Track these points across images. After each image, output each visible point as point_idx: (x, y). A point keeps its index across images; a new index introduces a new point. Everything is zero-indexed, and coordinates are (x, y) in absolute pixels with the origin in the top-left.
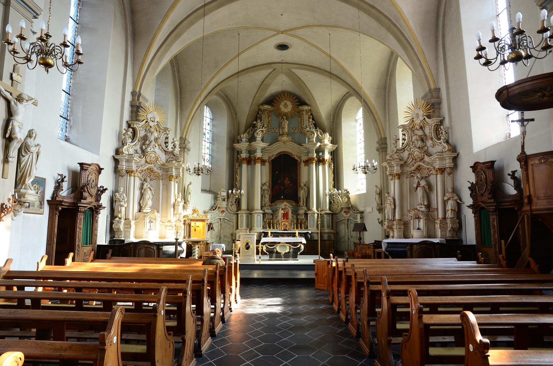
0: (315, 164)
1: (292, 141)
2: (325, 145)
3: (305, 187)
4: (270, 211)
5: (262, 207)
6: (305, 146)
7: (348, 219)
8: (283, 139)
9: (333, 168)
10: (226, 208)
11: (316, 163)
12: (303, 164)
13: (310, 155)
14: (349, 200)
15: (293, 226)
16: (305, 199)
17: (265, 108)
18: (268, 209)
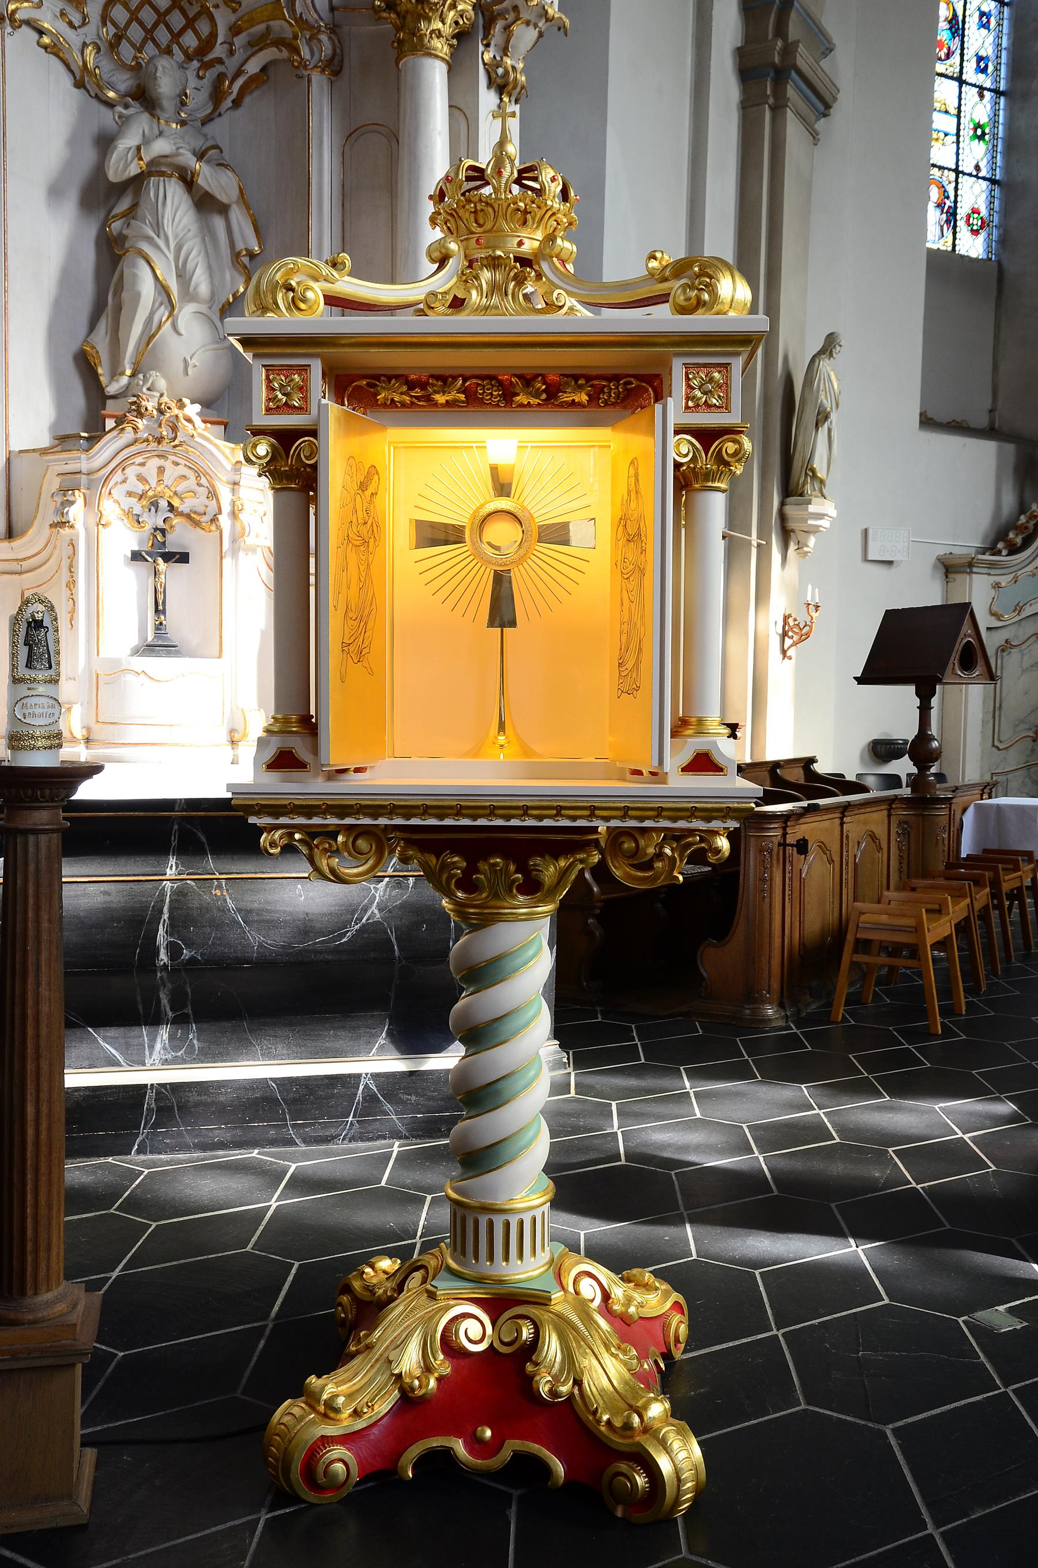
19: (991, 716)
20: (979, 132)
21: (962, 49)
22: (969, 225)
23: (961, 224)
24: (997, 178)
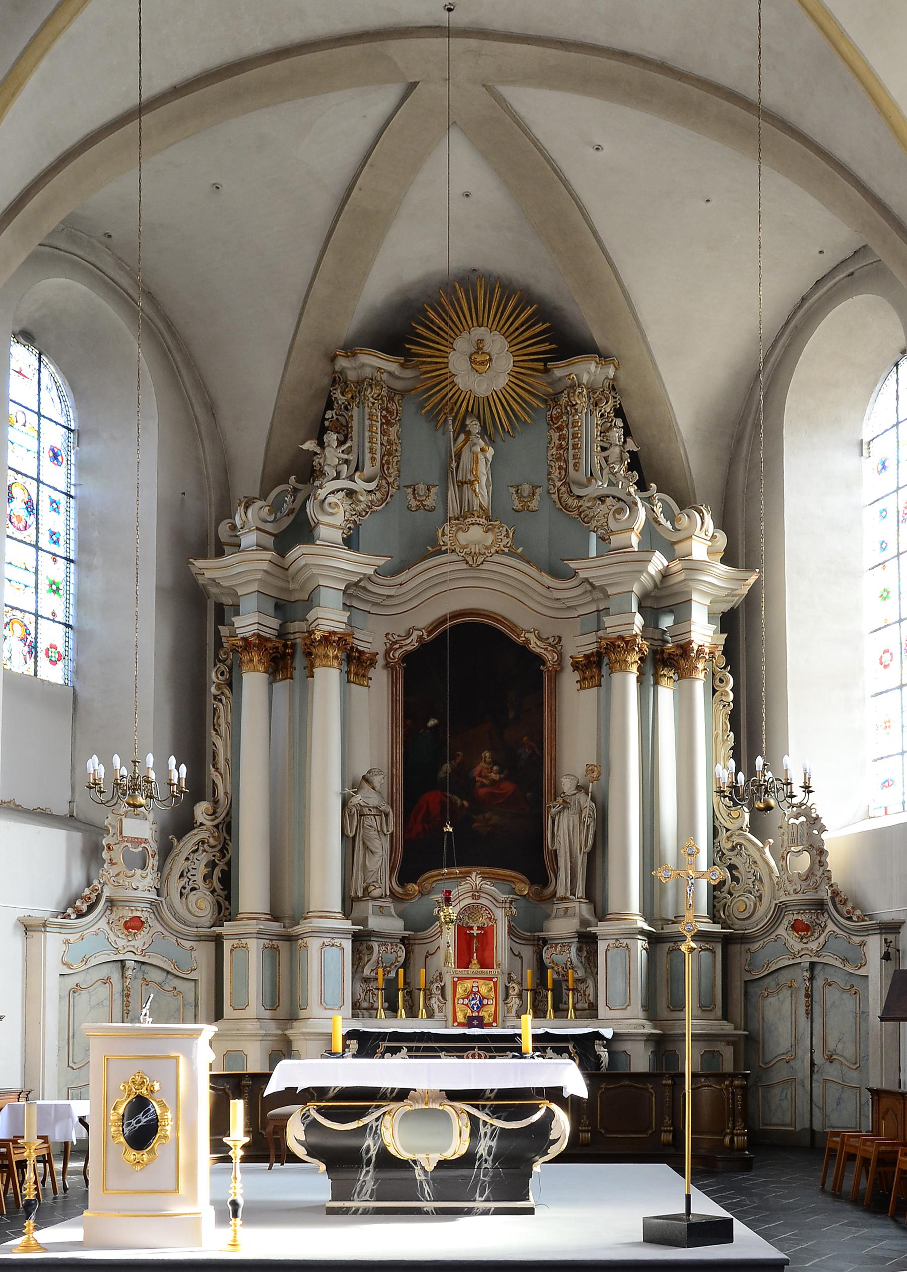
0: (634, 668)
2: (694, 568)
3: (582, 797)
4: (394, 925)
5: (349, 903)
6: (582, 574)
7: (813, 965)
9: (731, 696)
10: (155, 906)
11: (639, 669)
12: (570, 679)
13: (608, 621)
14: (822, 864)
15: (515, 1002)
16: (581, 861)
17: (368, 372)
18: (381, 912)
19: (66, 1042)
20: (54, 587)
21: (37, 524)
22: (48, 656)
23: (41, 655)
24: (70, 624)
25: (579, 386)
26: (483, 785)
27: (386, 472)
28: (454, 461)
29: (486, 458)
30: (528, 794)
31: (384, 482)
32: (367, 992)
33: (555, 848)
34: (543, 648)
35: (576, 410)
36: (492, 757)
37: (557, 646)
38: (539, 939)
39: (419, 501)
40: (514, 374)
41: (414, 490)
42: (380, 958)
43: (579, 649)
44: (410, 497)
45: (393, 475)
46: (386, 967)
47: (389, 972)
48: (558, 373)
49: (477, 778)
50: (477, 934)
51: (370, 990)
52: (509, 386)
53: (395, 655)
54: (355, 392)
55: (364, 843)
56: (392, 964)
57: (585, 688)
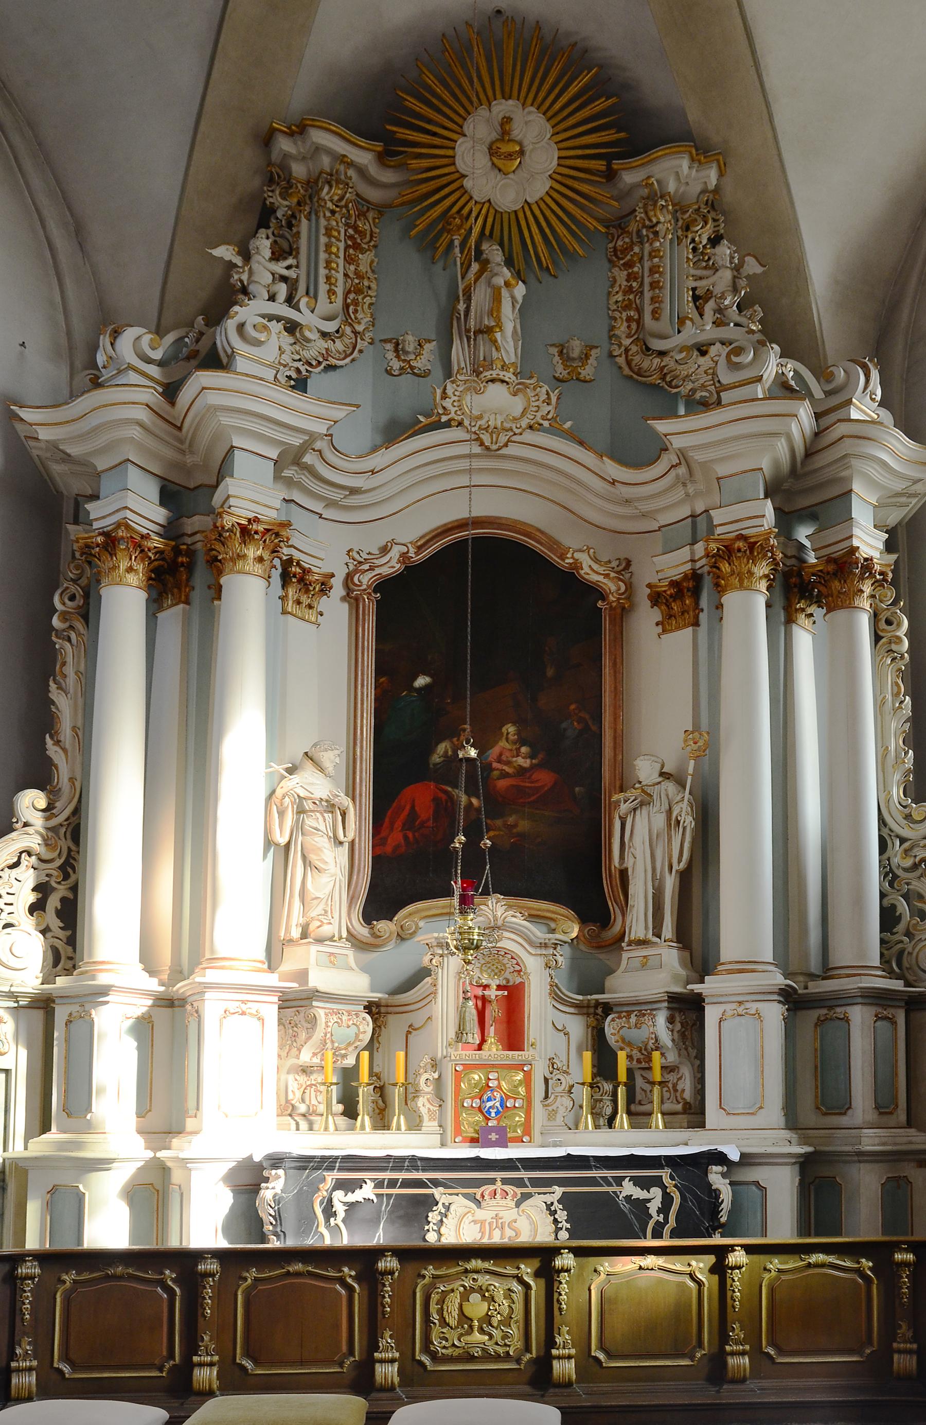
1: (555, 430)
8: (474, 403)
25: (662, 197)
26: (505, 775)
27: (353, 316)
28: (461, 302)
29: (513, 297)
30: (577, 789)
31: (348, 330)
32: (305, 1089)
33: (625, 865)
34: (603, 574)
35: (656, 233)
36: (518, 733)
37: (623, 573)
38: (598, 1004)
39: (404, 361)
40: (558, 177)
41: (397, 344)
42: (329, 1035)
43: (660, 576)
44: (391, 355)
45: (364, 322)
46: (339, 1049)
47: (344, 1056)
48: (629, 178)
49: (495, 765)
50: (496, 996)
51: (311, 1085)
52: (551, 197)
53: (363, 581)
54: (304, 196)
55: (304, 857)
56: (349, 1044)
57: (671, 631)
